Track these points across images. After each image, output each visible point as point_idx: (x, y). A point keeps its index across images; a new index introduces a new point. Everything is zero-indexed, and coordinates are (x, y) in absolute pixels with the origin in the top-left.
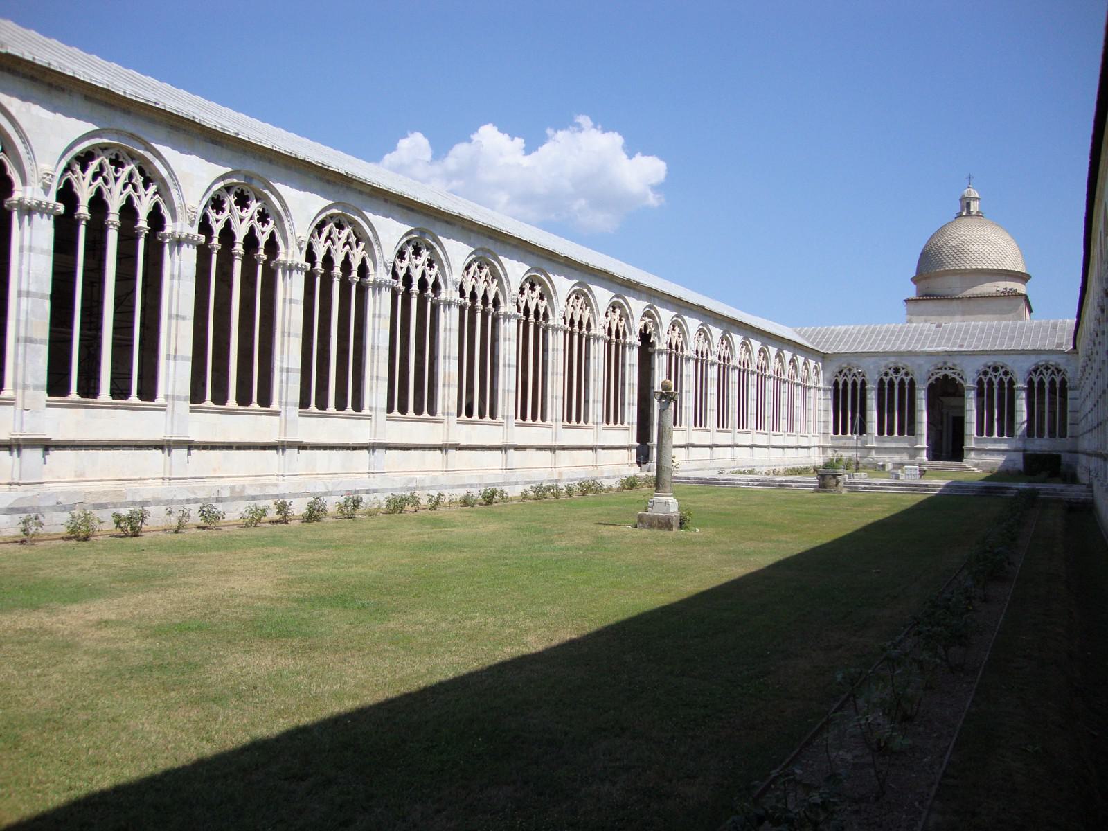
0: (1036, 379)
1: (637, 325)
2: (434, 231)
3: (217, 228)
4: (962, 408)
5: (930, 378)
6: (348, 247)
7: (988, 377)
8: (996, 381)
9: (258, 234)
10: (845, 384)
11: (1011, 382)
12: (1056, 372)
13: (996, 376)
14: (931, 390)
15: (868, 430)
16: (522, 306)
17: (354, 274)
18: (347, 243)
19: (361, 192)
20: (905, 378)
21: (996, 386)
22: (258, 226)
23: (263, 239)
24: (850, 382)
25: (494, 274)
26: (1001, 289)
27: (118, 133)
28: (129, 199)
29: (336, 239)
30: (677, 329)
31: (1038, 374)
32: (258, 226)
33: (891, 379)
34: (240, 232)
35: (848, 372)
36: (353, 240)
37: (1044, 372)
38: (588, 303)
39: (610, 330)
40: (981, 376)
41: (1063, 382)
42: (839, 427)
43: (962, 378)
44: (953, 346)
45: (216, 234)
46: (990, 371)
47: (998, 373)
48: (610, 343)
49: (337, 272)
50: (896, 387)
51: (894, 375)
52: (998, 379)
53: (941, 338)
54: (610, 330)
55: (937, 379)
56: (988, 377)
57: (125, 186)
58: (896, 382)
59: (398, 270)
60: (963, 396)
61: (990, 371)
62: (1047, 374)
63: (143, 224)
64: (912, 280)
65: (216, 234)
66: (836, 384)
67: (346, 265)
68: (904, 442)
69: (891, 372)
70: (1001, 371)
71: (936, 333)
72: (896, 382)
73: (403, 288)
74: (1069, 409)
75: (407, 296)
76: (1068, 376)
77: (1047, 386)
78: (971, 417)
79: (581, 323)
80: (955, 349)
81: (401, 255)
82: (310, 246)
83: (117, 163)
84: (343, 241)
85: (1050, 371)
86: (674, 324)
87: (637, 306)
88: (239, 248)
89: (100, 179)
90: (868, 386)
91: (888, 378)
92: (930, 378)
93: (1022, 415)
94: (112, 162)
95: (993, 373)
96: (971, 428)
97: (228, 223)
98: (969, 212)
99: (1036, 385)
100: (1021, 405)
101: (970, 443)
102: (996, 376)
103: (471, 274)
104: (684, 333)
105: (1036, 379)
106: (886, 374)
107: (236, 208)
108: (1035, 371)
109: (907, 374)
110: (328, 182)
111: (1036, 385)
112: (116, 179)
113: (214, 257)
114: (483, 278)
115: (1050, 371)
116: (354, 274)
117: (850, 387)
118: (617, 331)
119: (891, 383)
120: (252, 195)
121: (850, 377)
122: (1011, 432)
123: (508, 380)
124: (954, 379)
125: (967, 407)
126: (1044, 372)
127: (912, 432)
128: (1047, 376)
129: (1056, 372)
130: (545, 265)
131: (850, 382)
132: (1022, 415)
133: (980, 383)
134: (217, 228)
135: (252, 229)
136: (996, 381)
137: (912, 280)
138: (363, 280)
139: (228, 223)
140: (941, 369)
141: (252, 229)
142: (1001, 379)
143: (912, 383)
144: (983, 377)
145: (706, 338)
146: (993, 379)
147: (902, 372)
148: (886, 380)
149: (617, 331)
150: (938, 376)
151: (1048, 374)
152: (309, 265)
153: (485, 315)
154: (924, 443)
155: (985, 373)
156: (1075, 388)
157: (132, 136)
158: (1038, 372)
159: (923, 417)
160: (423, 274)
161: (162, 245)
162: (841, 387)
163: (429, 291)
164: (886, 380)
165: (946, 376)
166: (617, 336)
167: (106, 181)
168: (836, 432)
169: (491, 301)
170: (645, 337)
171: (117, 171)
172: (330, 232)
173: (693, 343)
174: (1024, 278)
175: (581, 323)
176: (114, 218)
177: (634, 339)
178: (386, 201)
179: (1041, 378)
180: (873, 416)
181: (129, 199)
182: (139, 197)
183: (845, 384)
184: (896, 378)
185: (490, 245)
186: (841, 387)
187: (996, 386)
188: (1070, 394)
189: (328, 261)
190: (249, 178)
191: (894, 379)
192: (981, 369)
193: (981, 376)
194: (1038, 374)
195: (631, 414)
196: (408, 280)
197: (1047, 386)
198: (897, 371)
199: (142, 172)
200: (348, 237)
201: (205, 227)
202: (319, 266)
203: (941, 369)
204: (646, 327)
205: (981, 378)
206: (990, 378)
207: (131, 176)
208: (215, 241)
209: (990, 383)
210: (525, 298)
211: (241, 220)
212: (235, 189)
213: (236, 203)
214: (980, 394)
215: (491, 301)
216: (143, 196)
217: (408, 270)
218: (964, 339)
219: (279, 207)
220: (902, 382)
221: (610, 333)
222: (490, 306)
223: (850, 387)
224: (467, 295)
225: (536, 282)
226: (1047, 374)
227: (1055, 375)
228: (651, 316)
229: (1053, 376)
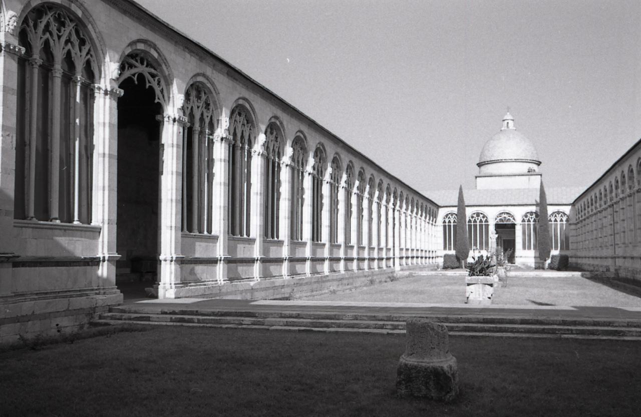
5: (496, 219)
7: (527, 218)
12: (563, 215)
13: (532, 218)
14: (498, 227)
20: (482, 219)
33: (475, 219)
35: (451, 216)
40: (524, 218)
43: (514, 219)
46: (529, 215)
47: (533, 216)
51: (477, 218)
56: (527, 218)
61: (529, 215)
64: (477, 164)
69: (475, 216)
85: (560, 215)
91: (473, 219)
92: (496, 219)
95: (530, 217)
101: (517, 253)
102: (532, 218)
106: (472, 217)
109: (483, 217)
115: (560, 215)
121: (452, 219)
126: (557, 215)
129: (563, 215)
137: (477, 164)
144: (525, 219)
147: (481, 216)
150: (501, 218)
155: (526, 216)
158: (554, 216)
168: (445, 248)
184: (478, 219)
191: (477, 220)
192: (524, 213)
193: (524, 218)
198: (478, 214)
205: (524, 219)
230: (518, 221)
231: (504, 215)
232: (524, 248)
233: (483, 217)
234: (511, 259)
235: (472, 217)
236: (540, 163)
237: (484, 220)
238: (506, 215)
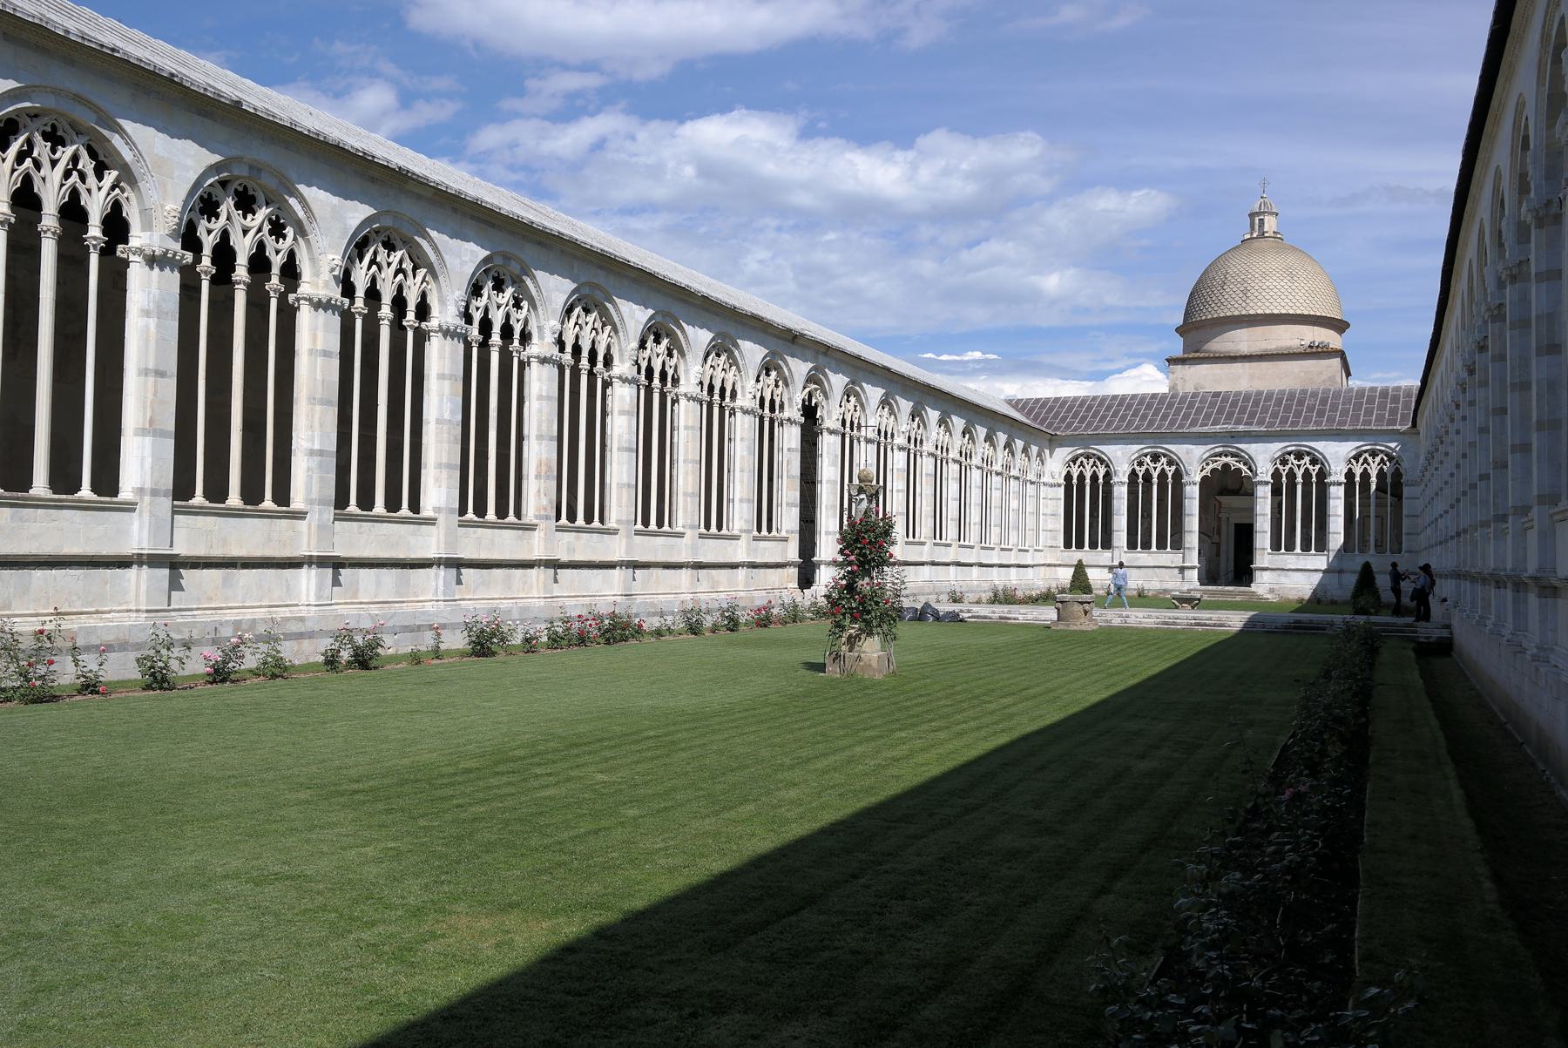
0: (1358, 471)
1: (799, 397)
2: (522, 256)
3: (208, 243)
4: (1251, 510)
6: (401, 276)
8: (1299, 474)
9: (269, 252)
10: (1081, 477)
11: (1322, 475)
15: (1116, 542)
16: (644, 365)
17: (411, 316)
18: (400, 271)
19: (419, 197)
21: (1299, 479)
22: (270, 242)
23: (277, 261)
24: (1088, 475)
25: (606, 319)
26: (1306, 343)
27: (56, 92)
28: (74, 193)
29: (385, 265)
30: (852, 399)
32: (270, 242)
34: (243, 248)
36: (408, 265)
37: (1370, 459)
38: (733, 362)
39: (762, 399)
41: (1397, 474)
42: (1072, 538)
44: (1238, 422)
45: (207, 251)
48: (762, 419)
49: (386, 311)
50: (1155, 480)
53: (1220, 411)
54: (762, 399)
55: (1213, 470)
57: (67, 174)
58: (1155, 475)
59: (472, 310)
60: (1251, 494)
63: (95, 231)
64: (1177, 330)
65: (207, 251)
66: (1068, 477)
67: (399, 303)
68: (1169, 557)
69: (1148, 459)
70: (1307, 459)
71: (1212, 405)
72: (1155, 475)
73: (481, 338)
74: (1405, 512)
75: (484, 346)
76: (1405, 465)
78: (1263, 525)
79: (723, 390)
80: (1241, 428)
81: (476, 290)
82: (347, 273)
83: (56, 140)
84: (394, 267)
85: (1378, 459)
86: (848, 394)
87: (799, 368)
88: (241, 273)
89: (28, 162)
90: (1115, 479)
93: (1337, 525)
94: (46, 136)
96: (1263, 539)
97: (225, 235)
98: (1262, 235)
99: (1357, 479)
100: (1337, 506)
103: (573, 320)
104: (862, 406)
105: (1358, 471)
106: (1140, 464)
107: (237, 215)
108: (1356, 458)
109: (1170, 463)
110: (373, 180)
111: (1357, 479)
112: (54, 163)
113: (205, 285)
114: (590, 326)
115: (1378, 459)
116: (411, 316)
117: (1088, 481)
118: (772, 402)
119: (1147, 477)
120: (261, 198)
122: (1322, 546)
123: (621, 470)
124: (1239, 470)
125: (1259, 509)
126: (1370, 459)
127: (1178, 545)
128: (1374, 466)
130: (676, 308)
131: (1088, 475)
132: (1337, 525)
133: (1276, 475)
134: (208, 243)
135: (261, 246)
136: (1299, 474)
137: (1177, 330)
138: (423, 325)
139: (225, 235)
140: (1220, 455)
141: (261, 246)
143: (1178, 475)
145: (892, 412)
147: (1164, 460)
148: (1141, 471)
149: (772, 402)
152: (347, 301)
153: (591, 374)
154: (1193, 559)
156: (1413, 484)
157: (78, 98)
159: (1192, 523)
160: (508, 316)
161: (126, 263)
162: (1075, 481)
163: (516, 343)
164: (1141, 471)
165: (1226, 466)
166: (772, 410)
167: (37, 165)
168: (1068, 545)
169: (600, 358)
170: (809, 411)
171: (54, 151)
172: (375, 253)
173: (874, 418)
174: (1340, 326)
175: (723, 390)
176: (49, 219)
177: (793, 412)
178: (455, 210)
180: (1120, 522)
181: (74, 193)
182: (89, 191)
183: (1081, 477)
185: (600, 278)
186: (1075, 481)
187: (1299, 479)
188: (1406, 491)
189: (373, 295)
190: (255, 168)
195: (788, 518)
196: (486, 326)
199: (93, 154)
200: (401, 262)
201: (190, 240)
202: (359, 302)
203: (1220, 455)
204: (810, 395)
207: (75, 159)
208: (206, 261)
209: (1291, 475)
210: (647, 353)
211: (245, 232)
212: (235, 185)
213: (237, 207)
214: (1276, 491)
215: (600, 358)
216: (94, 190)
217: (486, 310)
218: (1252, 415)
219: (301, 214)
220: (1163, 475)
221: (762, 406)
222: (600, 365)
223: (1088, 481)
224: (569, 349)
225: (663, 333)
228: (818, 382)
230: (1264, 471)
231: (1225, 459)
232: (1276, 546)
233: (1170, 463)
234: (1243, 574)
235: (1140, 464)
236: (1348, 325)
237: (1170, 471)
238: (1229, 460)
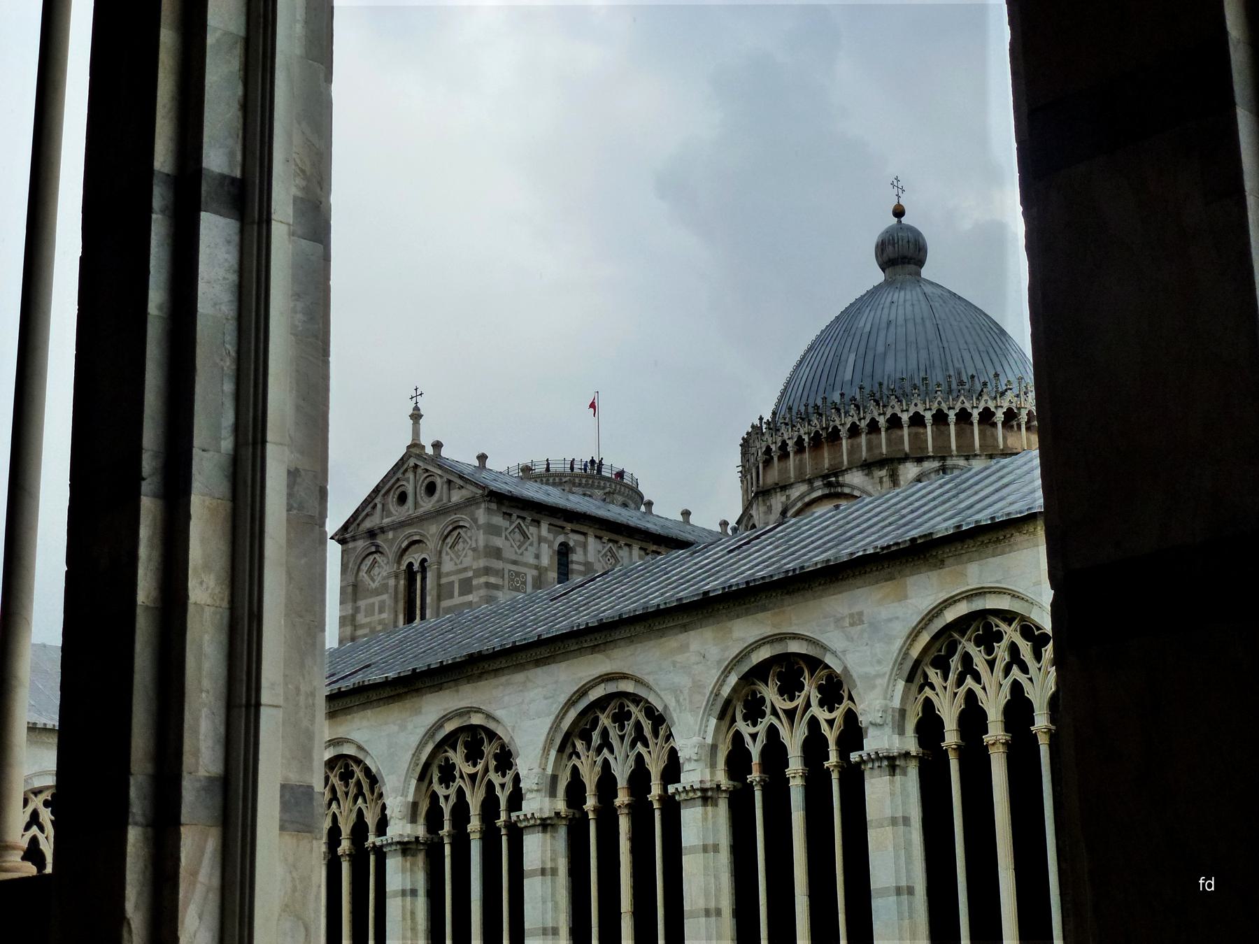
7: (762, 727)
31: (952, 676)
52: (801, 731)
62: (991, 664)
77: (995, 732)
136: (793, 740)
142: (814, 723)
146: (784, 732)
151: (999, 666)
179: (971, 695)
194: (952, 676)
197: (995, 732)
206: (772, 732)
226: (991, 664)
227: (1024, 669)
229: (969, 682)
